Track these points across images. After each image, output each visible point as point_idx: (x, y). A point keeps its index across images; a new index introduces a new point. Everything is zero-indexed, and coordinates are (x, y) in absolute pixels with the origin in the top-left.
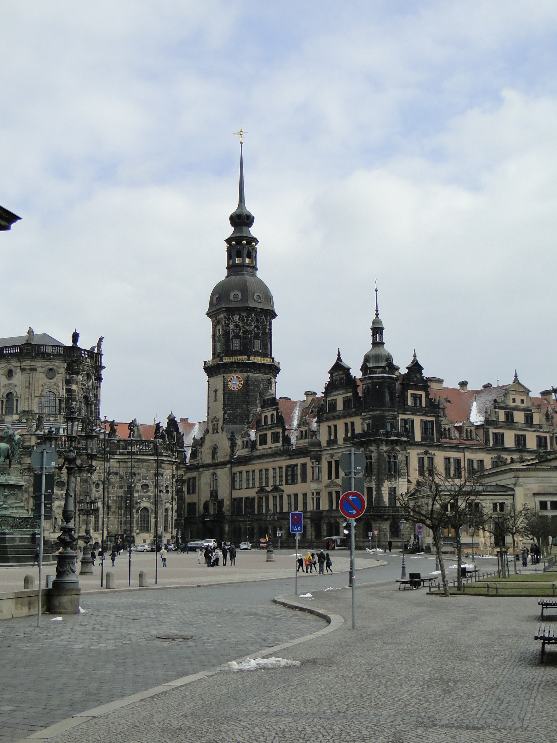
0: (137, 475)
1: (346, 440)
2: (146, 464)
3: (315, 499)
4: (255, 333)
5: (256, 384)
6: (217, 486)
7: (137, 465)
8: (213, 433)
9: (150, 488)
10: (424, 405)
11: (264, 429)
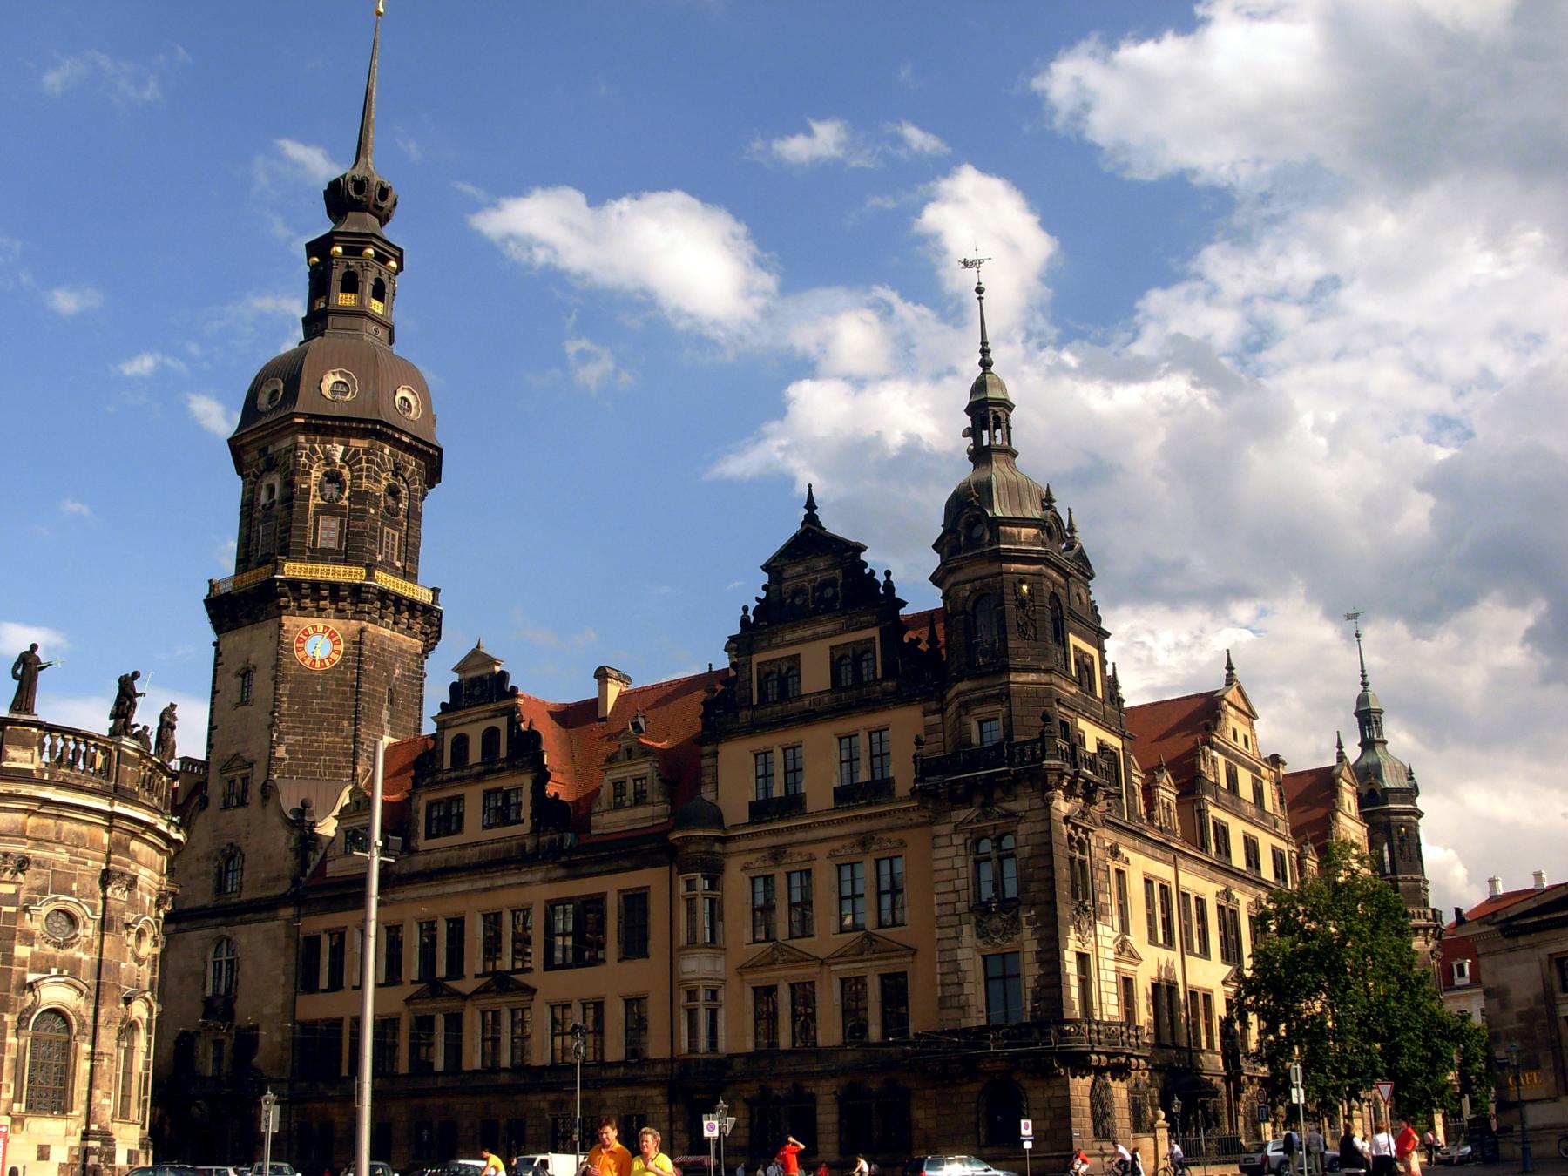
0: (33, 869)
1: (845, 795)
2: (75, 827)
3: (703, 1016)
4: (387, 508)
5: (384, 658)
6: (233, 981)
7: (36, 828)
8: (227, 806)
9: (80, 932)
10: (1099, 694)
11: (450, 780)
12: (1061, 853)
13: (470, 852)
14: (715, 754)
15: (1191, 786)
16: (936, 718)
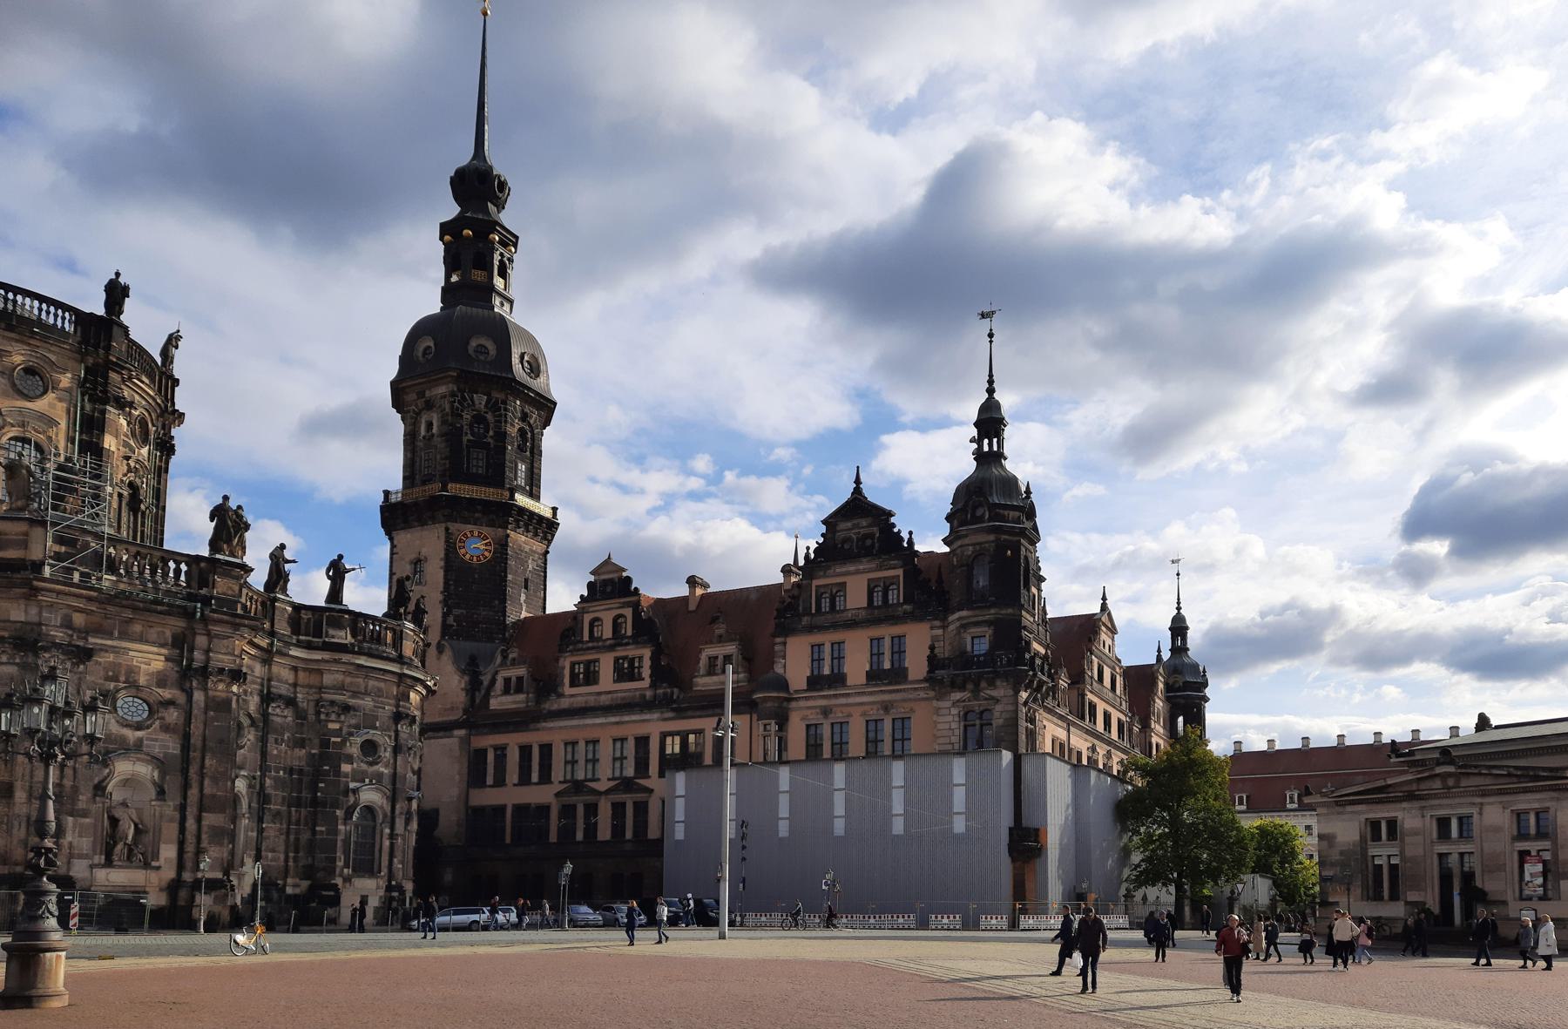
1: (875, 676)
2: (376, 683)
12: (1023, 724)
13: (603, 698)
14: (785, 644)
15: (1078, 679)
16: (940, 632)
